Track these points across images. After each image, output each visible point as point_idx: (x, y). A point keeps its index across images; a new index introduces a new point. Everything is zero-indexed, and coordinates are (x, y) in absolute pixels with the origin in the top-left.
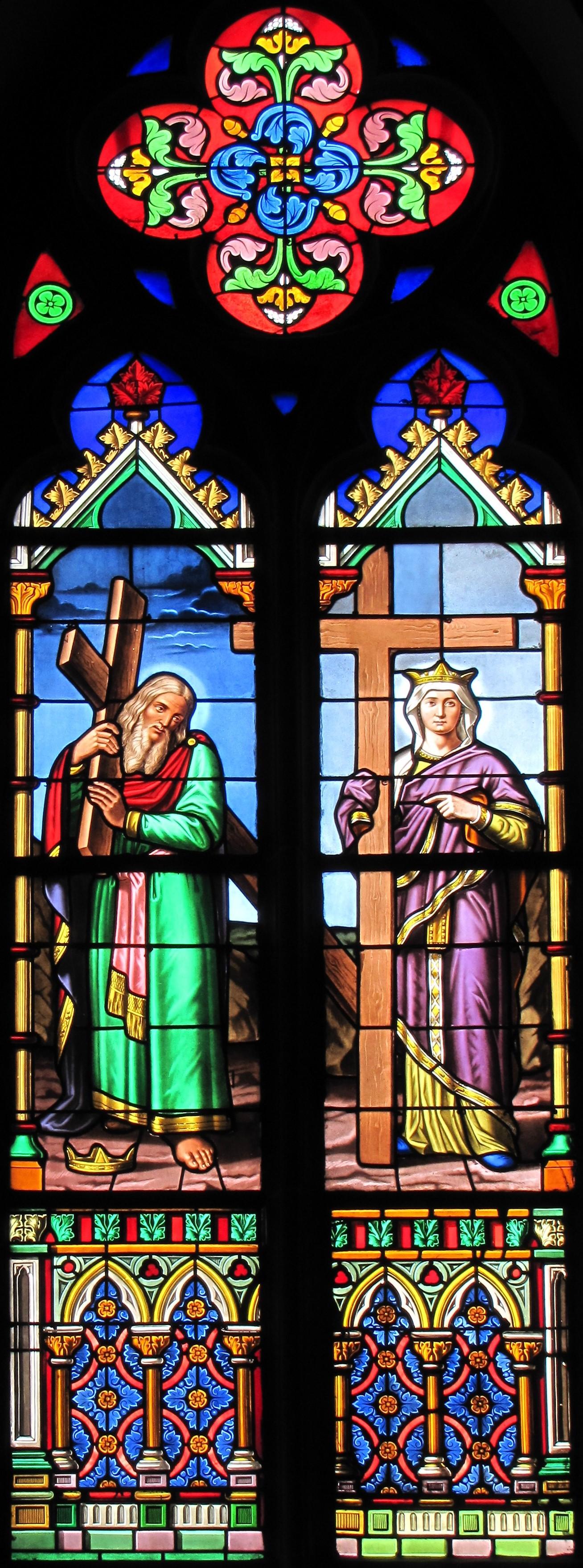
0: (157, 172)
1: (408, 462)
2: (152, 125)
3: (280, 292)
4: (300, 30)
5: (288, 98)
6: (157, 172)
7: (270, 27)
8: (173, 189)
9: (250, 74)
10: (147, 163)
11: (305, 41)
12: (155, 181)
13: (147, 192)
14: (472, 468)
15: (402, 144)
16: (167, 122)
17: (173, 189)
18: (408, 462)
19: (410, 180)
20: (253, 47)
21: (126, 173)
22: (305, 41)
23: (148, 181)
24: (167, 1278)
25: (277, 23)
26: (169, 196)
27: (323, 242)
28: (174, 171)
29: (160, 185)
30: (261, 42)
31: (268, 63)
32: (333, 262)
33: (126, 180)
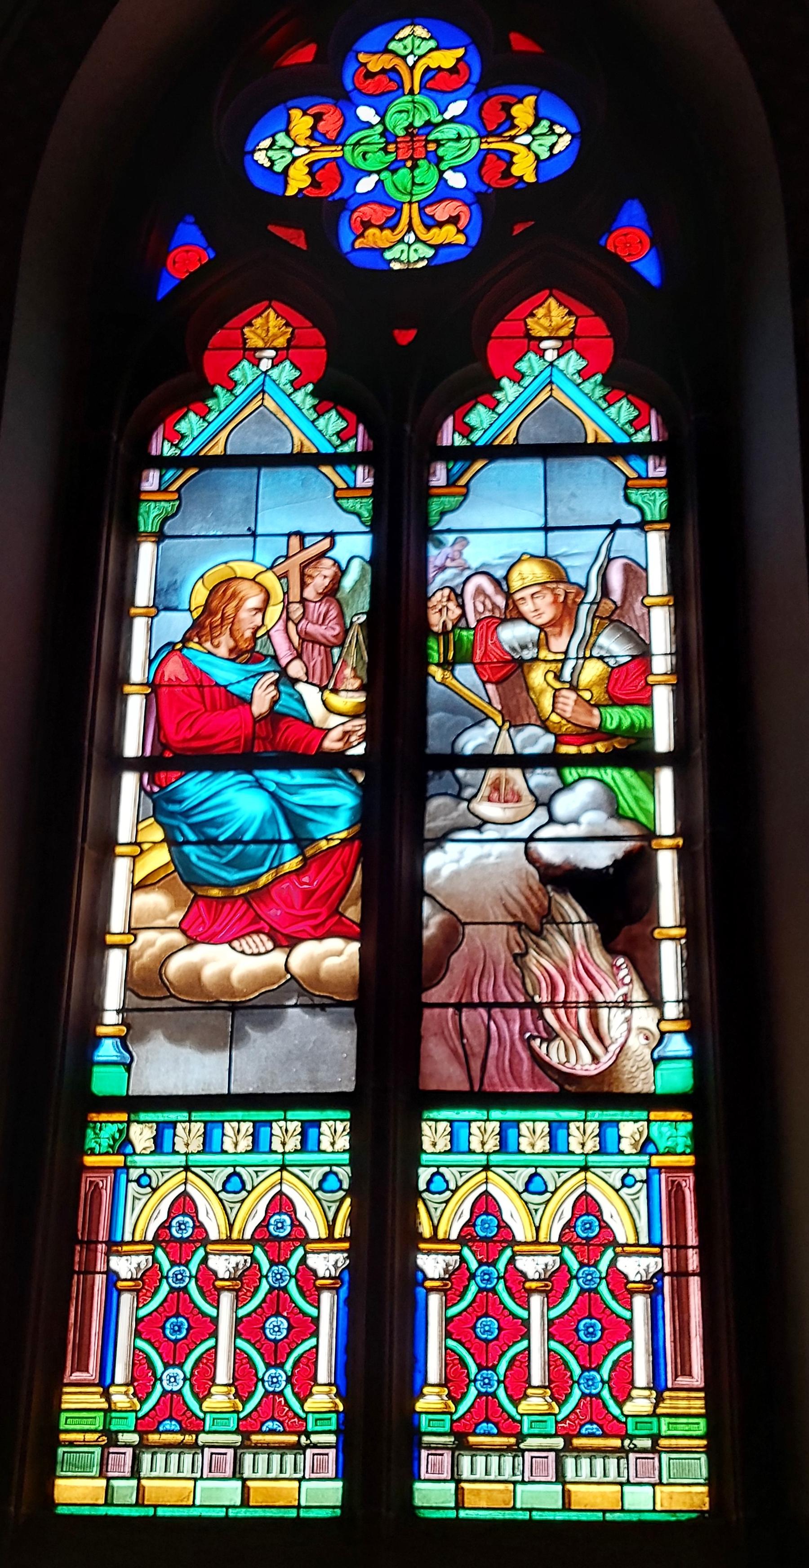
0: (297, 152)
1: (522, 390)
2: (296, 113)
3: (405, 247)
4: (428, 36)
5: (417, 89)
6: (297, 152)
7: (401, 35)
8: (310, 165)
9: (383, 71)
10: (290, 144)
11: (432, 44)
12: (295, 159)
13: (287, 168)
14: (583, 392)
15: (516, 122)
16: (308, 112)
17: (310, 165)
18: (522, 390)
19: (524, 151)
20: (386, 51)
21: (270, 153)
22: (432, 44)
23: (289, 158)
24: (249, 1192)
25: (407, 31)
26: (307, 170)
27: (444, 204)
28: (311, 149)
29: (299, 163)
30: (393, 46)
31: (397, 61)
32: (454, 220)
33: (270, 159)
